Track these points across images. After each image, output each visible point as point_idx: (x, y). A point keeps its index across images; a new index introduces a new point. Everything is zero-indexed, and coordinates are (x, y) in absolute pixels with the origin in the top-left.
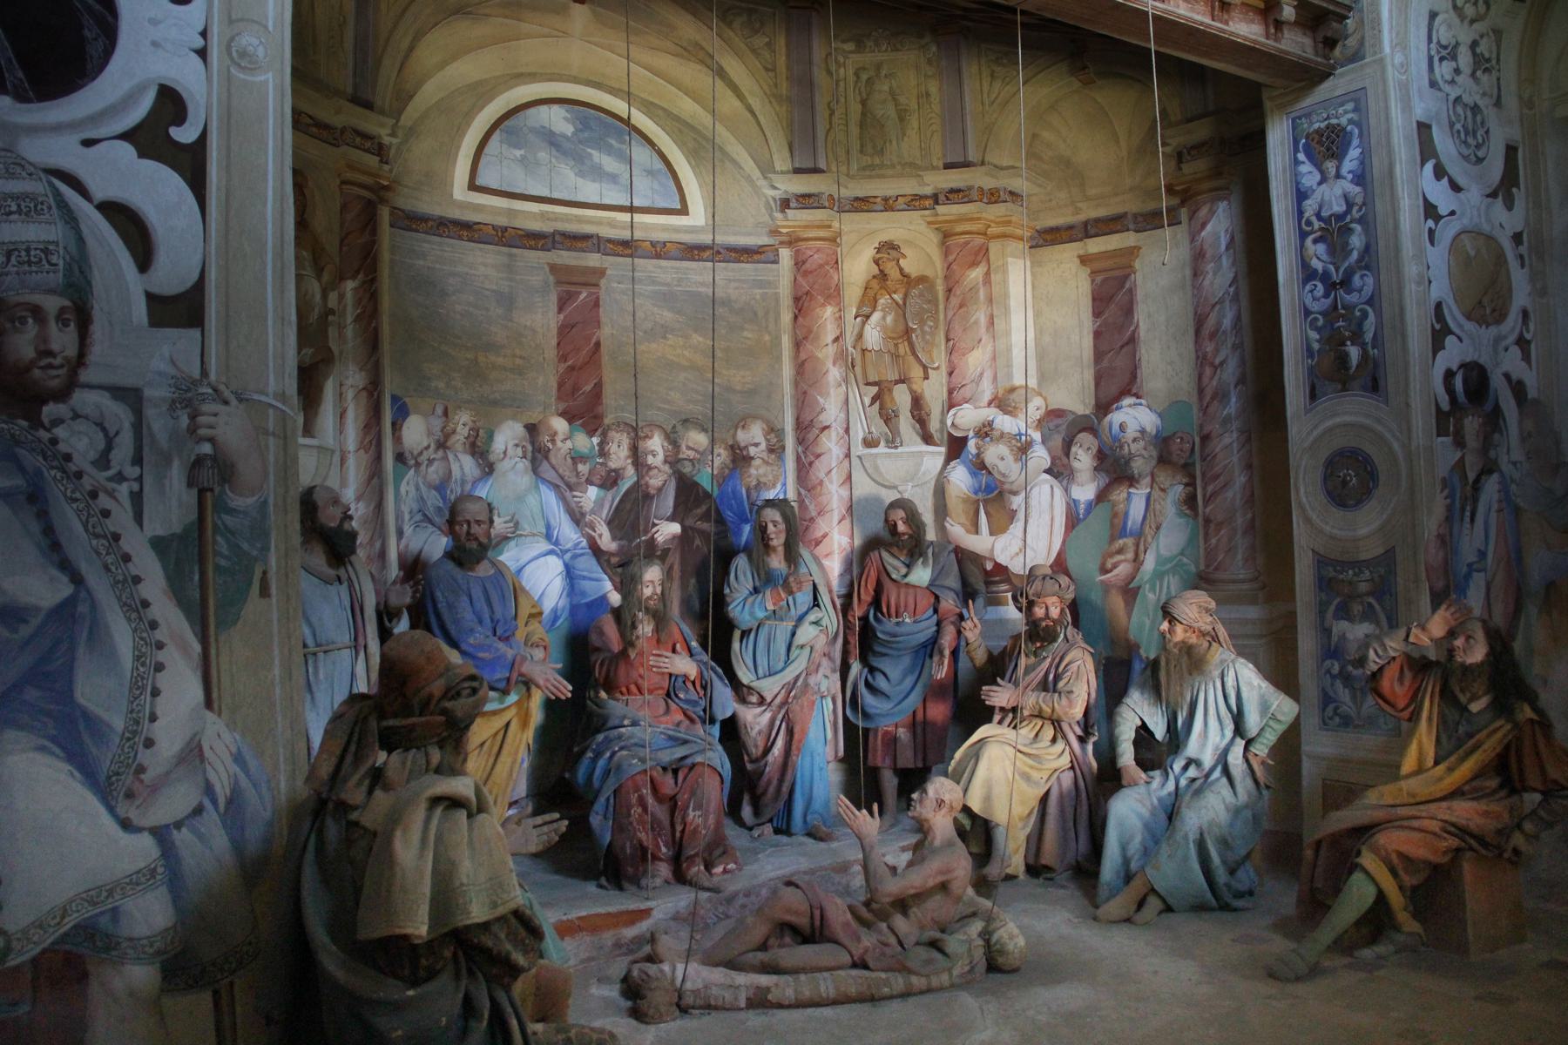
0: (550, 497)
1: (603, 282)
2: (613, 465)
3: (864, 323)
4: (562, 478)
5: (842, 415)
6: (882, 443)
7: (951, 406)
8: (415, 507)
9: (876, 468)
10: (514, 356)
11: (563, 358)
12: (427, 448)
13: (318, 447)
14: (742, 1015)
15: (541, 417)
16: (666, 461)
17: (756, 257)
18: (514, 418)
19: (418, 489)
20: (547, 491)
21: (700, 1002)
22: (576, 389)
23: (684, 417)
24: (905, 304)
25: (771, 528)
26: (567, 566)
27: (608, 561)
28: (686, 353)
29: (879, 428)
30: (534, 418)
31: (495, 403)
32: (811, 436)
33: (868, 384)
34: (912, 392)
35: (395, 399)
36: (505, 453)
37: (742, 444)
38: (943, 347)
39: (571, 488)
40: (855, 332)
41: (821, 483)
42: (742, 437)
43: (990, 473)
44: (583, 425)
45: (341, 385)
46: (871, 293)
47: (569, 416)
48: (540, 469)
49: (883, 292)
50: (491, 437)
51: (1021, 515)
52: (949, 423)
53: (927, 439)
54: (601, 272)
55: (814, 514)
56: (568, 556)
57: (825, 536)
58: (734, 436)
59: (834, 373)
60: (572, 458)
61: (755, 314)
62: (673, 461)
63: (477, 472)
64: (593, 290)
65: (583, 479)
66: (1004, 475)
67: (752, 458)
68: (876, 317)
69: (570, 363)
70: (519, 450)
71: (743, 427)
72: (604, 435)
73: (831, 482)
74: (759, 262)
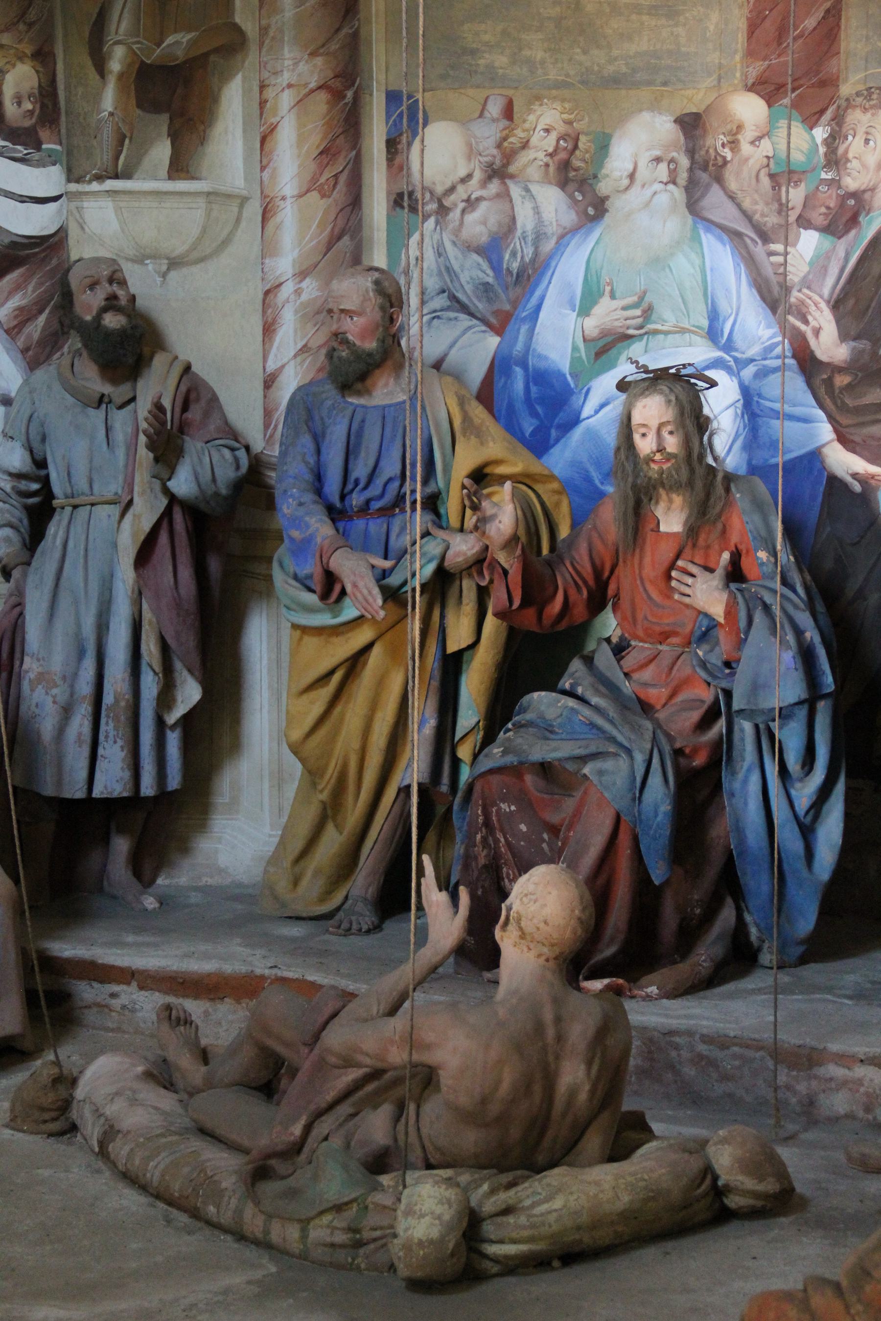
2: (851, 183)
4: (748, 216)
8: (432, 283)
12: (469, 176)
13: (209, 194)
18: (655, 106)
19: (440, 252)
20: (718, 246)
26: (746, 393)
27: (829, 383)
31: (616, 81)
35: (393, 98)
36: (632, 176)
39: (765, 237)
44: (795, 105)
45: (262, 87)
48: (706, 202)
50: (603, 147)
56: (748, 372)
60: (772, 176)
63: (569, 217)
65: (793, 217)
70: (663, 168)
72: (838, 120)
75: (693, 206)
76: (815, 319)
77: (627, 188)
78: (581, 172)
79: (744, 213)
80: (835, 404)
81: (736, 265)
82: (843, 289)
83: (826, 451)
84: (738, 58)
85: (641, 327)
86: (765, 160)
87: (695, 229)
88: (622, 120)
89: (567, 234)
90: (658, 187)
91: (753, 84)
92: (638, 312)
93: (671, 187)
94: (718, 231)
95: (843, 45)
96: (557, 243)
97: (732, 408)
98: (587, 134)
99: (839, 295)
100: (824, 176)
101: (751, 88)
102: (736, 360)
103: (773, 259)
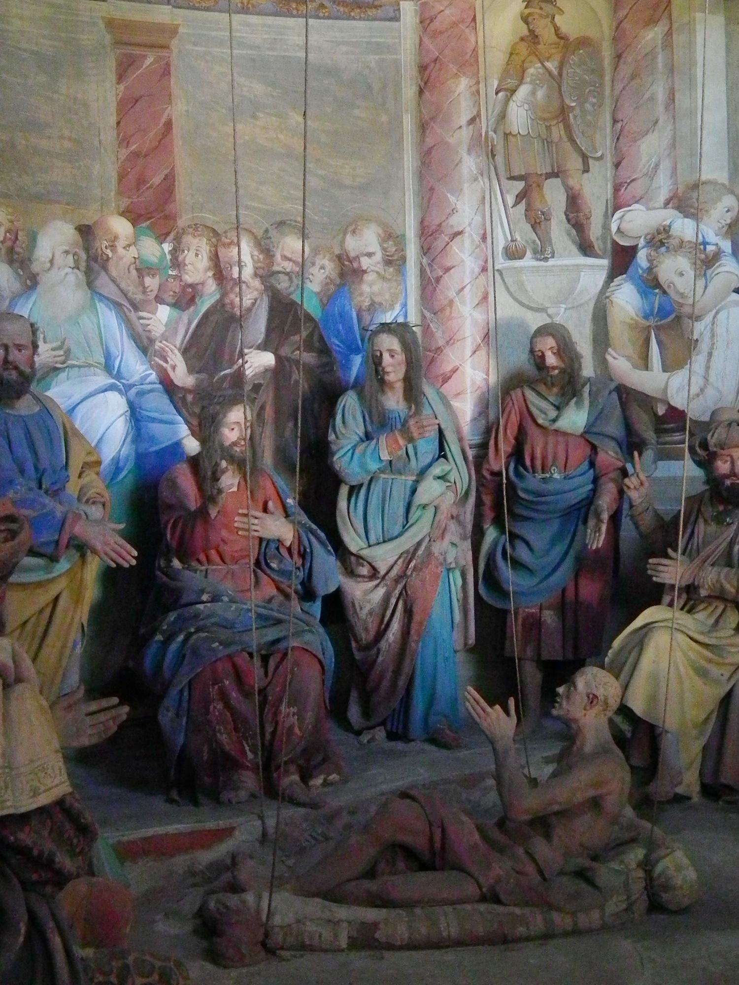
0: (110, 319)
1: (174, 43)
2: (189, 279)
3: (507, 100)
5: (478, 218)
6: (529, 254)
7: (617, 207)
9: (520, 284)
10: (62, 137)
11: (124, 141)
14: (341, 958)
15: (96, 218)
16: (256, 275)
17: (371, 13)
21: (291, 940)
22: (141, 181)
23: (278, 219)
24: (560, 74)
25: (386, 357)
26: (132, 406)
27: (184, 399)
28: (281, 137)
29: (524, 234)
30: (89, 216)
31: (39, 198)
32: (439, 244)
33: (512, 178)
34: (568, 189)
36: (52, 261)
37: (352, 254)
38: (608, 130)
40: (498, 109)
41: (451, 302)
42: (352, 245)
43: (665, 292)
44: (151, 228)
46: (517, 60)
47: (134, 216)
49: (535, 59)
51: (704, 347)
52: (614, 228)
53: (586, 248)
54: (173, 31)
55: (441, 343)
56: (133, 391)
57: (455, 370)
58: (342, 242)
59: (469, 164)
60: (137, 270)
61: (369, 87)
62: (266, 275)
63: (16, 286)
64: (164, 53)
65: (152, 296)
66: (682, 295)
67: (364, 272)
68: (523, 91)
69: (133, 148)
70: (70, 257)
71: (354, 232)
72: (178, 240)
73: (463, 303)
74: (375, 19)
75: (90, 284)
76: (172, 360)
77: (49, 270)
78: (22, 255)
79: (122, 291)
80: (188, 412)
81: (120, 324)
82: (188, 342)
83: (185, 442)
84: (113, 194)
85: (64, 363)
86: (133, 259)
87: (92, 299)
88: (44, 223)
89: (16, 297)
90: (69, 270)
91: (123, 212)
92: (61, 352)
93: (76, 271)
94: (106, 301)
95: (178, 197)
96: (10, 303)
97: (123, 417)
98: (23, 230)
99: (186, 345)
100: (170, 272)
101: (123, 214)
102: (124, 385)
103: (142, 321)
